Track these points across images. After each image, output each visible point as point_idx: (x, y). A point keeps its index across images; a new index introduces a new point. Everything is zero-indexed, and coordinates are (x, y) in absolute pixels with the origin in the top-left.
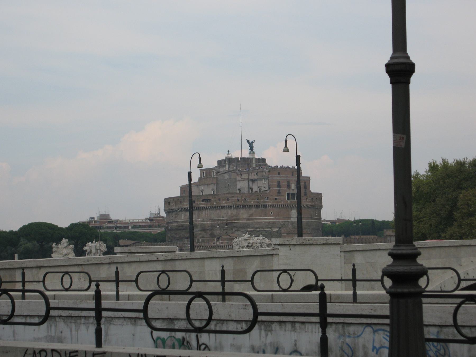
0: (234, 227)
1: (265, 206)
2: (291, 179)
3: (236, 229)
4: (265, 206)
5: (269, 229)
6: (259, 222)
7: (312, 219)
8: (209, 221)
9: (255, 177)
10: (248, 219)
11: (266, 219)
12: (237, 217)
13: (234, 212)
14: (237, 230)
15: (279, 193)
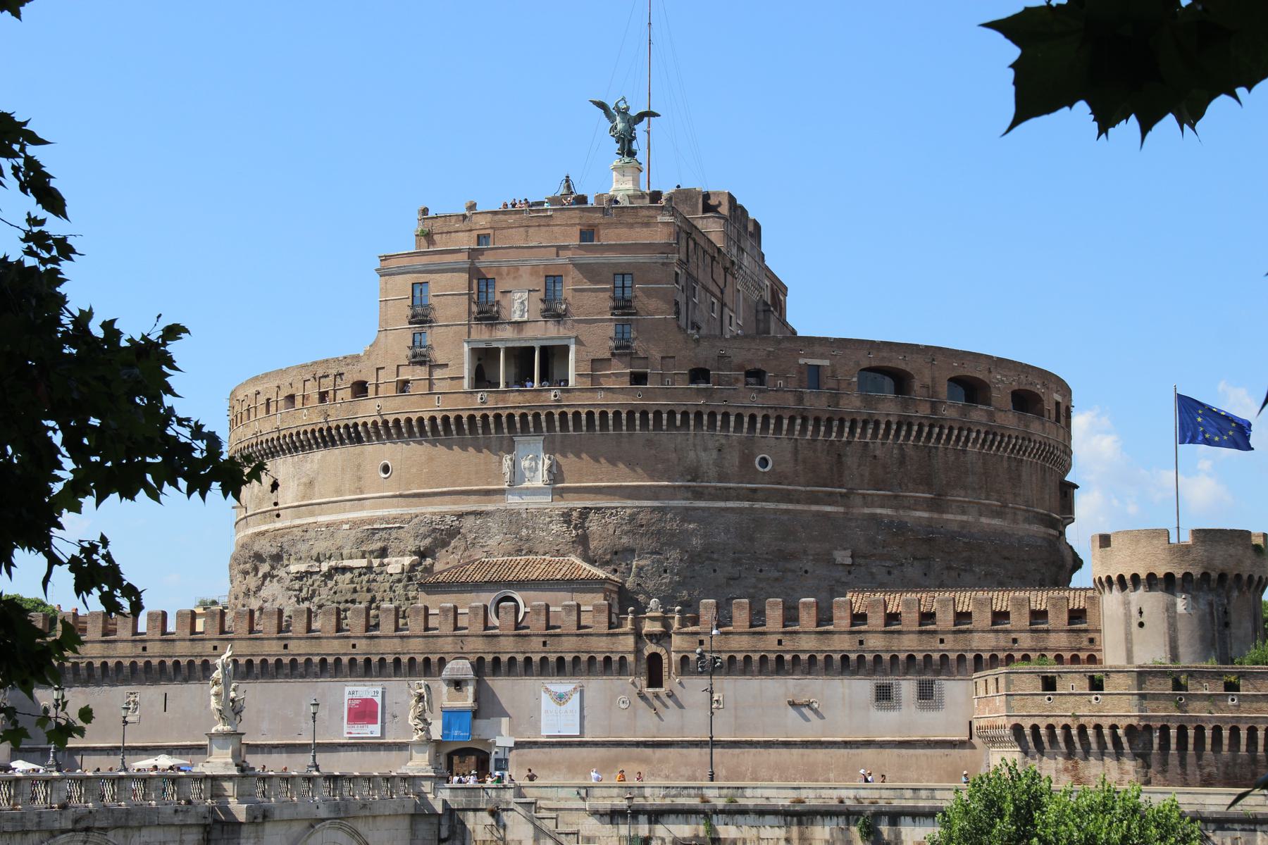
0: (258, 557)
4: (354, 435)
6: (328, 526)
7: (698, 494)
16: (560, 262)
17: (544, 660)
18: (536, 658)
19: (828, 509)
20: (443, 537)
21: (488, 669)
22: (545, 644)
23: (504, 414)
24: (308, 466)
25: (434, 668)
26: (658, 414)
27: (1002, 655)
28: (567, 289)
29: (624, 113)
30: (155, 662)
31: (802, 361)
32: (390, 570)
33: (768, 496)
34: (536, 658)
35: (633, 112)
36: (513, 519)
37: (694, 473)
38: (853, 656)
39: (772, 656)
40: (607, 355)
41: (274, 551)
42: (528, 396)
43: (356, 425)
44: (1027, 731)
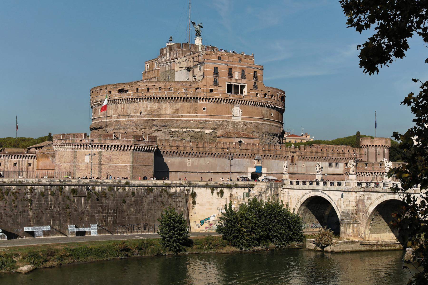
0: (154, 125)
1: (196, 99)
2: (234, 65)
3: (157, 128)
4: (196, 99)
5: (199, 130)
6: (185, 120)
7: (264, 120)
8: (125, 117)
9: (191, 64)
10: (173, 116)
11: (197, 116)
12: (158, 112)
13: (155, 105)
14: (158, 130)
15: (216, 82)
18: (272, 155)
19: (278, 125)
20: (219, 126)
24: (177, 105)
27: (349, 158)
28: (246, 73)
30: (195, 152)
32: (206, 132)
36: (234, 123)
39: (314, 157)
40: (252, 89)
41: (164, 125)
42: (238, 96)
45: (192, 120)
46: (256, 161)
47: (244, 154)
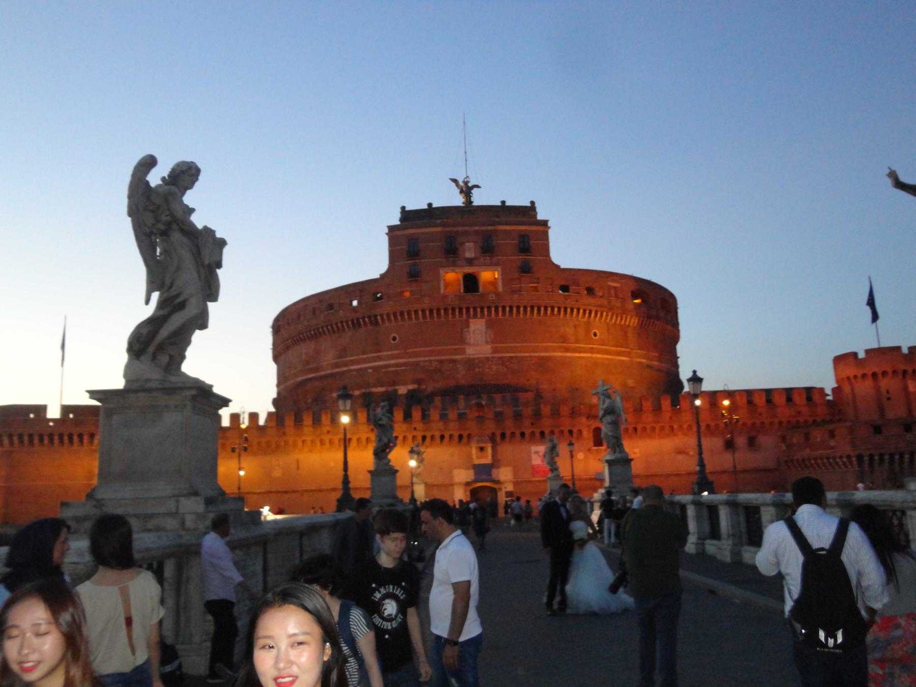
2: (460, 229)
10: (337, 365)
11: (379, 358)
16: (490, 228)
17: (533, 433)
21: (498, 438)
22: (532, 424)
23: (464, 306)
25: (465, 440)
26: (546, 308)
29: (466, 183)
31: (610, 283)
33: (599, 352)
34: (527, 432)
35: (470, 185)
36: (471, 364)
37: (564, 339)
38: (712, 424)
43: (376, 316)
44: (866, 458)
45: (370, 368)
46: (474, 451)
47: (438, 435)
